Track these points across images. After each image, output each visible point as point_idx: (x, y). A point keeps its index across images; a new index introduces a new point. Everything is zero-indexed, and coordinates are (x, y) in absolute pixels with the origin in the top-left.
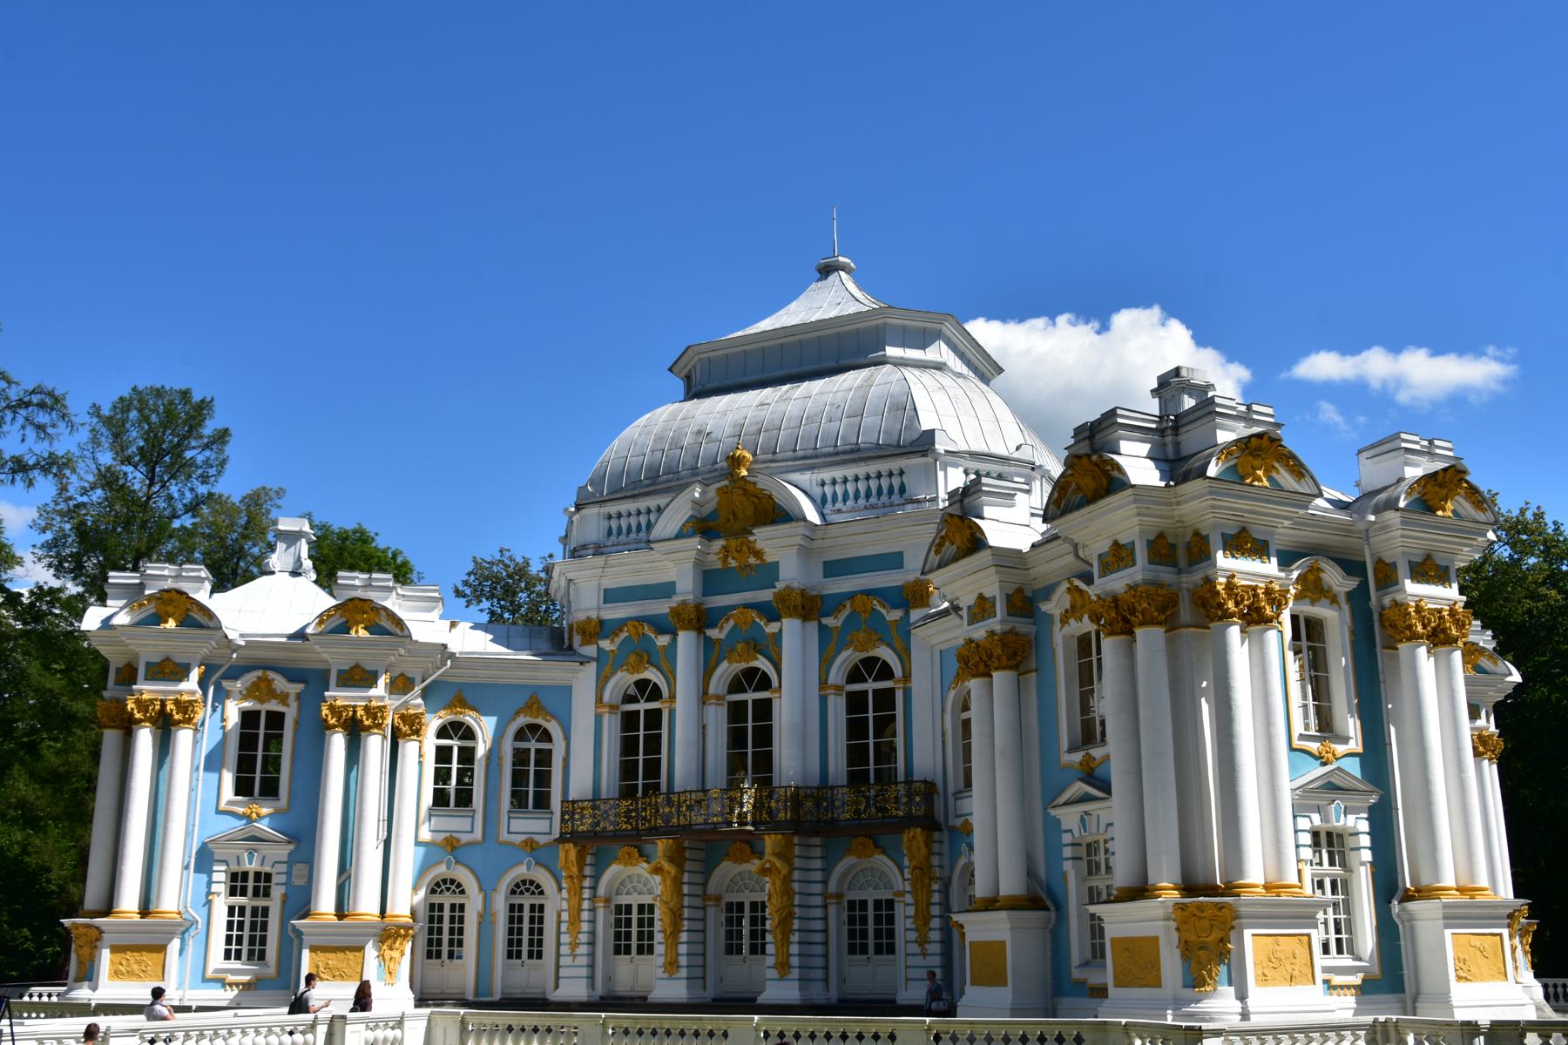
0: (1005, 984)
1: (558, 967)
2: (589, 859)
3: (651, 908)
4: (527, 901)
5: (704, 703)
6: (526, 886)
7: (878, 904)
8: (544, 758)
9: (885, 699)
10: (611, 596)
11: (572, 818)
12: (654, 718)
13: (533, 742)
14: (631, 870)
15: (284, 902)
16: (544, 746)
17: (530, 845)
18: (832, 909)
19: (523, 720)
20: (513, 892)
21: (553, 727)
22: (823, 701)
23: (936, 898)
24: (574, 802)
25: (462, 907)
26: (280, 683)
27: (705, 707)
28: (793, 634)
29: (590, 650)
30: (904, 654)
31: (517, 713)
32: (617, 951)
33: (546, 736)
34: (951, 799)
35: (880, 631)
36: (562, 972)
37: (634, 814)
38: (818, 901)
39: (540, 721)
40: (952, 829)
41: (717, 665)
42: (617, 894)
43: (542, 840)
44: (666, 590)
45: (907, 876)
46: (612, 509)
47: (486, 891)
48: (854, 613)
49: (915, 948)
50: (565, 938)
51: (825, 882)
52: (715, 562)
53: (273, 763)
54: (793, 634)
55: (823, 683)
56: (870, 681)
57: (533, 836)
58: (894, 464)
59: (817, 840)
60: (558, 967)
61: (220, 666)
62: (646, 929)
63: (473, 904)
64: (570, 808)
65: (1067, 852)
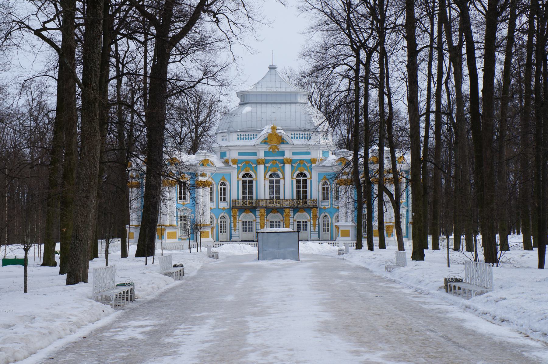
4: (223, 220)
6: (223, 217)
7: (303, 222)
8: (225, 189)
9: (305, 181)
10: (240, 154)
12: (251, 182)
14: (247, 214)
16: (224, 187)
17: (224, 209)
18: (295, 223)
21: (227, 183)
22: (292, 181)
23: (317, 221)
28: (288, 167)
29: (235, 166)
31: (221, 180)
33: (225, 185)
34: (320, 202)
35: (306, 168)
36: (232, 235)
38: (293, 221)
40: (320, 208)
41: (268, 172)
44: (255, 154)
45: (312, 216)
46: (239, 134)
47: (217, 219)
48: (299, 163)
49: (313, 230)
50: (233, 228)
52: (267, 150)
54: (288, 167)
55: (292, 177)
59: (293, 209)
63: (215, 221)
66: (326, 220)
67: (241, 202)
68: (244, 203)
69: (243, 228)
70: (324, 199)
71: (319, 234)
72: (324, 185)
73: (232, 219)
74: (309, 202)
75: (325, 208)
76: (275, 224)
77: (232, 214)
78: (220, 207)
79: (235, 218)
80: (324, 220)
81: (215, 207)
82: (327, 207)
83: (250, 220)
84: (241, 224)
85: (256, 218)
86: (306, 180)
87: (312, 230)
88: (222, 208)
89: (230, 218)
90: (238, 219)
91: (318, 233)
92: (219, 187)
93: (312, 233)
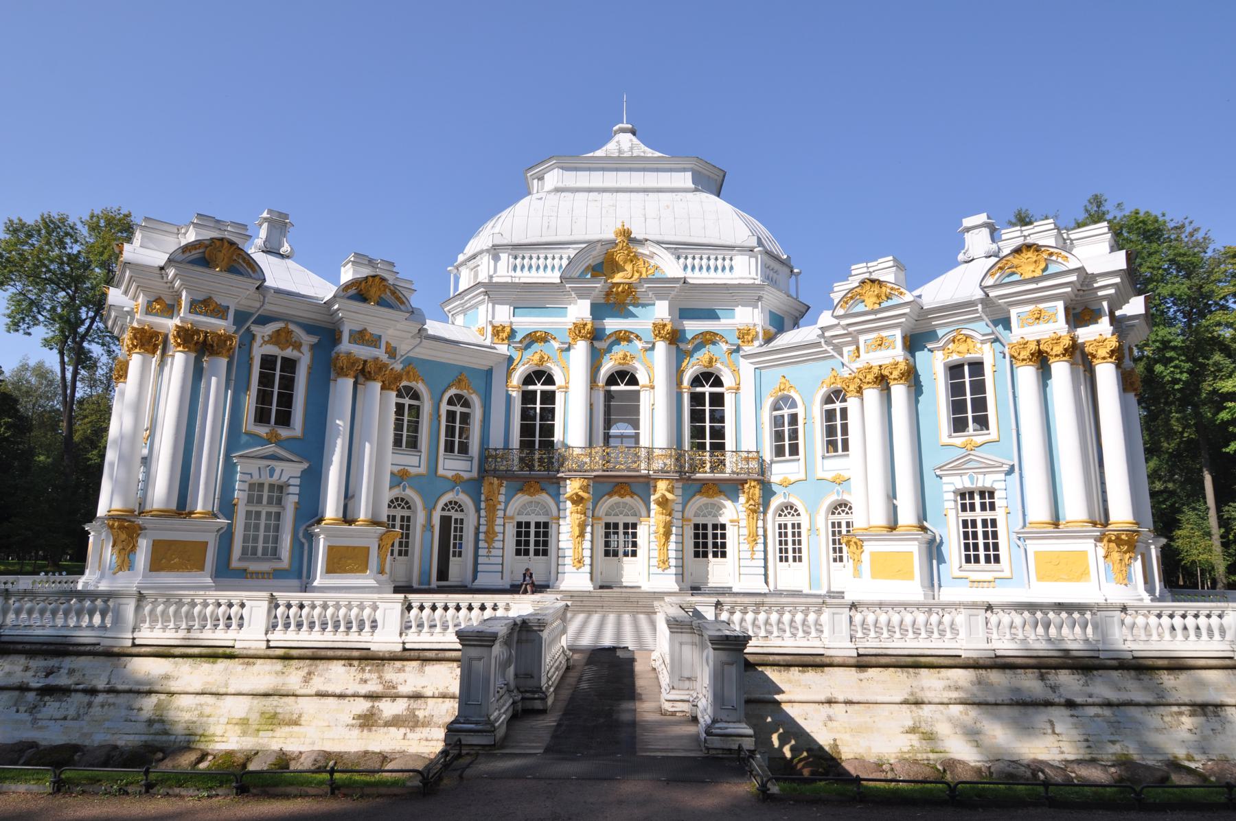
0: (911, 578)
1: (476, 564)
2: (503, 490)
3: (546, 525)
5: (591, 389)
8: (465, 418)
9: (718, 400)
11: (496, 461)
13: (459, 406)
15: (296, 509)
16: (465, 410)
17: (456, 481)
19: (453, 391)
20: (443, 509)
24: (496, 450)
25: (409, 518)
26: (299, 334)
27: (593, 391)
30: (736, 372)
32: (518, 553)
33: (466, 404)
36: (480, 568)
37: (546, 460)
39: (464, 392)
42: (518, 514)
43: (466, 475)
49: (748, 555)
50: (482, 544)
51: (683, 512)
53: (286, 400)
56: (707, 387)
57: (459, 472)
58: (728, 254)
60: (476, 564)
61: (251, 314)
62: (541, 539)
63: (420, 518)
64: (486, 455)
65: (951, 496)
66: (789, 520)
67: (515, 456)
68: (521, 460)
69: (518, 543)
70: (779, 451)
71: (766, 567)
72: (776, 407)
73: (483, 513)
74: (730, 459)
75: (786, 484)
76: (621, 530)
77: (483, 498)
78: (441, 472)
79: (492, 509)
80: (782, 520)
81: (422, 470)
82: (793, 478)
83: (542, 519)
84: (511, 531)
85: (559, 510)
86: (721, 396)
87: (743, 555)
88: (450, 474)
89: (478, 510)
90: (500, 514)
91: (762, 563)
92: (444, 408)
93: (743, 563)
